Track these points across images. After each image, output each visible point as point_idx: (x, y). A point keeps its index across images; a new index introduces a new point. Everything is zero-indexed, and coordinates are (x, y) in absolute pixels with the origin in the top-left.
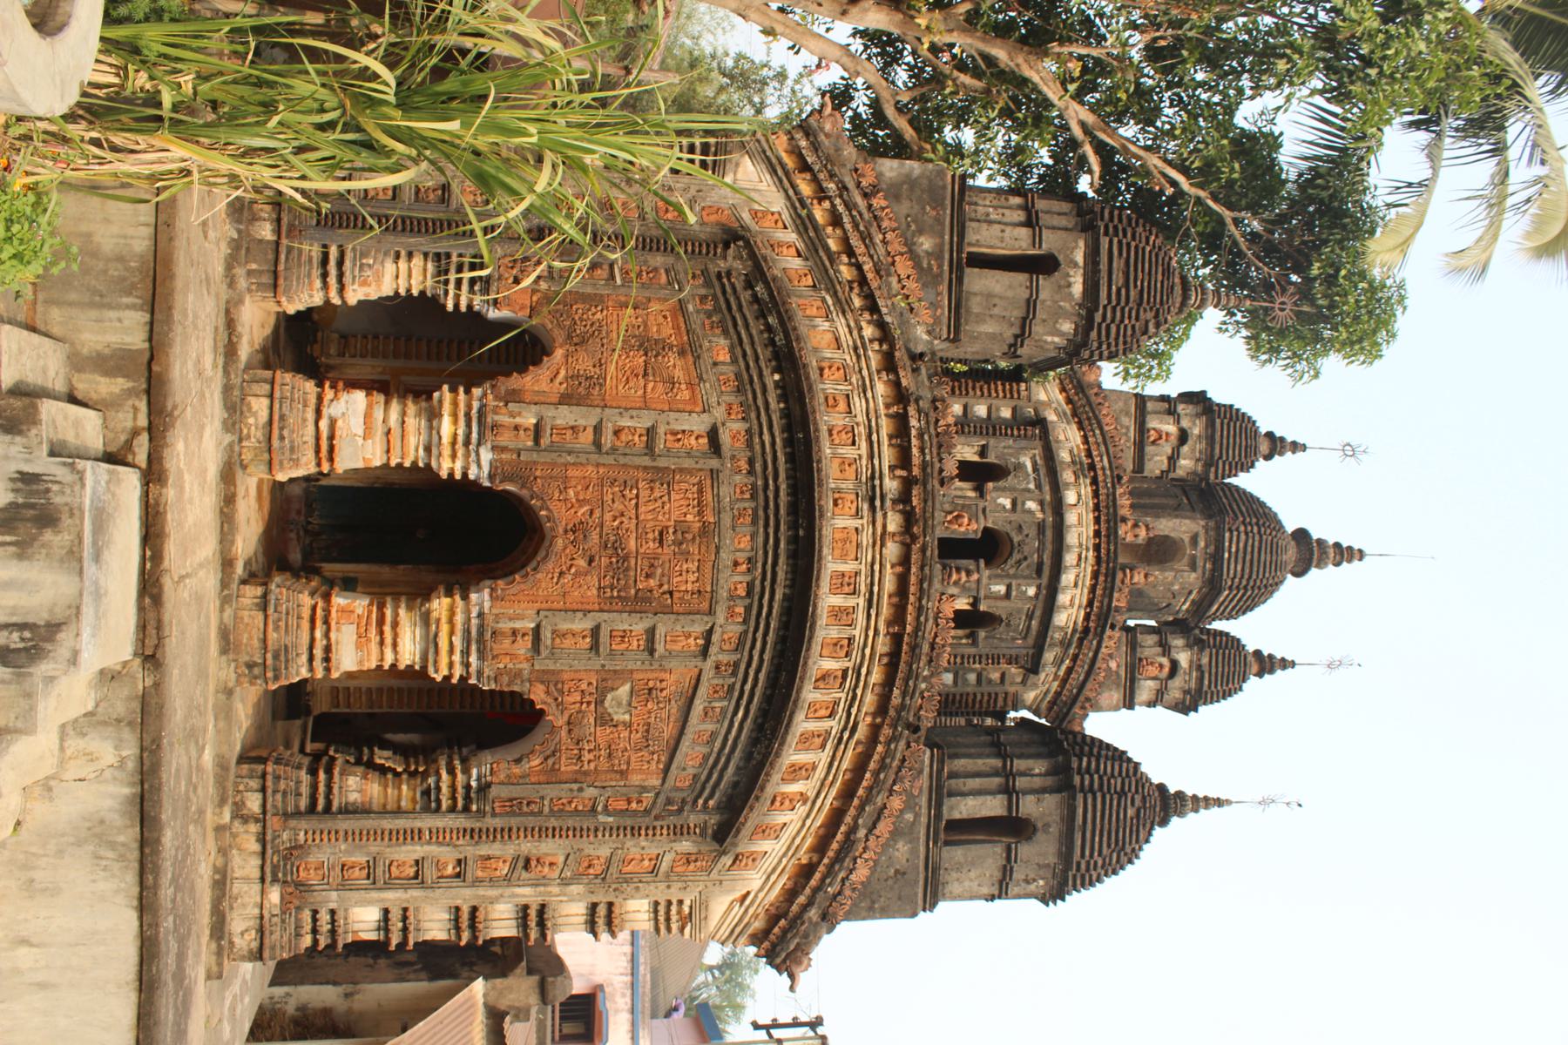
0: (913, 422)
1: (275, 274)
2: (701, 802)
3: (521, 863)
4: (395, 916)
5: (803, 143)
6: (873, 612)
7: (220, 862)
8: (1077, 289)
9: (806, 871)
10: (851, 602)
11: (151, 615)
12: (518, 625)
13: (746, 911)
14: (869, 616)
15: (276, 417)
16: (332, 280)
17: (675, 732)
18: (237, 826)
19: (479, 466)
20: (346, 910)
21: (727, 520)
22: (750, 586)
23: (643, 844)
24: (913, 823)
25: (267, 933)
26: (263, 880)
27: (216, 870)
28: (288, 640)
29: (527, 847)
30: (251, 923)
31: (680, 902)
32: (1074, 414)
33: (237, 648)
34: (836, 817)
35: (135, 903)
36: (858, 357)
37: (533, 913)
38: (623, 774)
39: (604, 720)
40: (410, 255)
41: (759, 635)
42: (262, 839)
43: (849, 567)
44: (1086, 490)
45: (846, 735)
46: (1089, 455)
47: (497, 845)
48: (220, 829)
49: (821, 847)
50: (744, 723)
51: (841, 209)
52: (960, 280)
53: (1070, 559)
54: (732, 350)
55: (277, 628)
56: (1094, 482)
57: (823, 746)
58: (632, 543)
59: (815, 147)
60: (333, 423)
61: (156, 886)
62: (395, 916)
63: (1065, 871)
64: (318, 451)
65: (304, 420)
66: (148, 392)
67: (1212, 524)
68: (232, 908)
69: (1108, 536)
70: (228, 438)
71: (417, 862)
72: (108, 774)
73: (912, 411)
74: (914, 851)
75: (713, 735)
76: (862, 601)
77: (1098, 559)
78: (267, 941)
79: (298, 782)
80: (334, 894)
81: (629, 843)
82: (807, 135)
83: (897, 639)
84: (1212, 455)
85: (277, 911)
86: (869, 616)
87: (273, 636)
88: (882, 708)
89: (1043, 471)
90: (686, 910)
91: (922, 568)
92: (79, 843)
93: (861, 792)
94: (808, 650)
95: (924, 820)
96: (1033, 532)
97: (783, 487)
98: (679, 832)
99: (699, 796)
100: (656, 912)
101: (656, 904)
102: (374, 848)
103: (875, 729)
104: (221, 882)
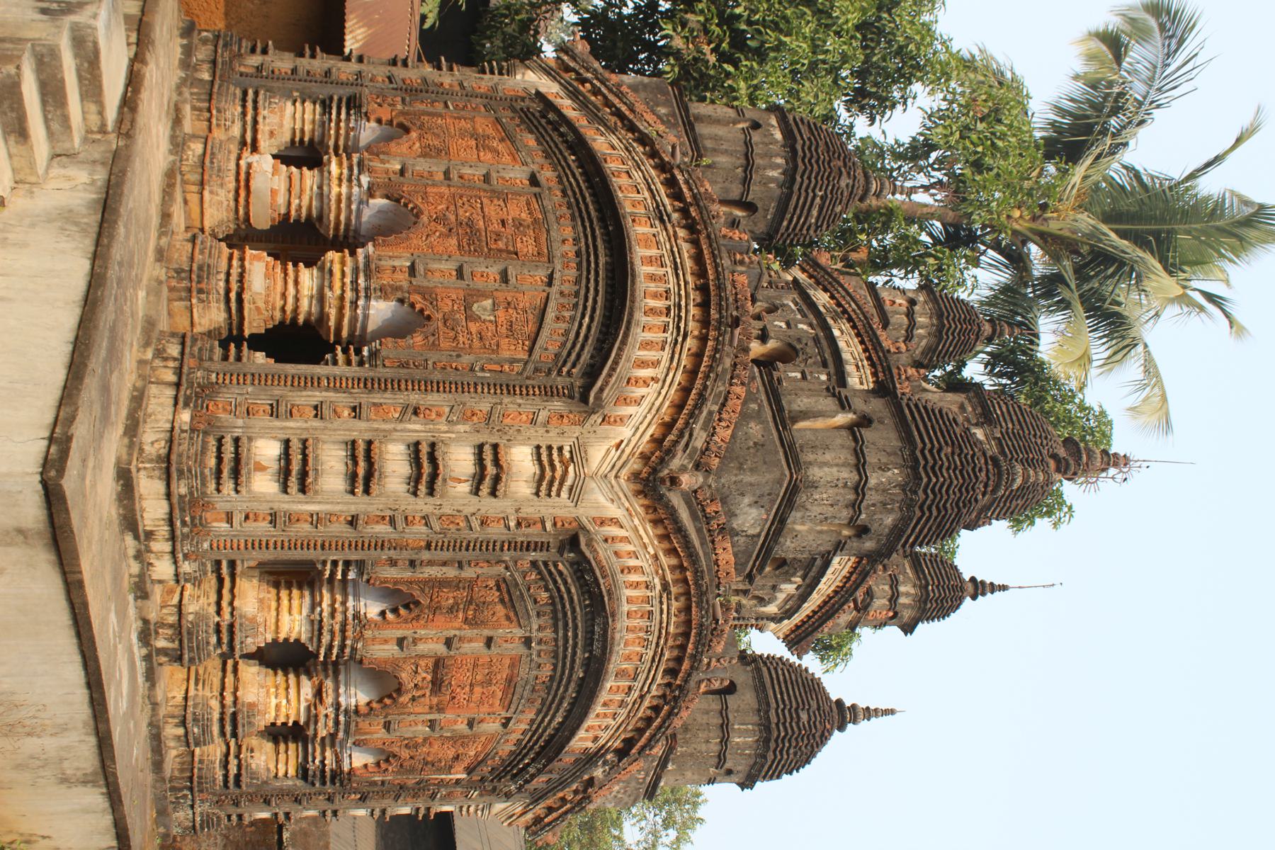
0: (679, 177)
1: (211, 95)
2: (565, 370)
3: (410, 410)
4: (296, 446)
5: (565, 58)
6: (680, 273)
7: (139, 384)
8: (778, 136)
9: (668, 427)
10: (661, 271)
11: (128, 116)
12: (397, 263)
13: (623, 451)
14: (677, 275)
15: (209, 151)
16: (250, 105)
17: (534, 329)
18: (158, 363)
19: (360, 186)
20: (250, 439)
21: (551, 217)
22: (578, 254)
23: (520, 401)
24: (759, 411)
25: (176, 442)
26: (176, 404)
27: (135, 388)
28: (211, 262)
29: (414, 398)
30: (162, 435)
31: (560, 449)
32: (818, 283)
33: (169, 260)
34: (685, 391)
35: (90, 255)
36: (630, 152)
37: (424, 449)
38: (496, 352)
39: (470, 317)
40: (303, 102)
41: (592, 277)
42: (179, 372)
43: (654, 252)
44: (846, 326)
45: (680, 339)
46: (839, 305)
47: (388, 395)
48: (142, 363)
49: (679, 407)
50: (591, 324)
51: (598, 84)
52: (693, 129)
53: (850, 368)
54: (537, 140)
55: (202, 252)
56: (850, 320)
57: (663, 349)
58: (481, 223)
59: (574, 58)
60: (249, 166)
61: (109, 246)
62: (296, 446)
63: (913, 453)
64: (237, 180)
65: (229, 160)
66: (139, 31)
67: (971, 394)
68: (145, 422)
69: (875, 349)
70: (172, 158)
71: (316, 407)
72: (80, 187)
73: (676, 172)
74: (766, 429)
75: (567, 332)
76: (669, 270)
77: (873, 365)
78: (175, 448)
79: (212, 350)
80: (240, 422)
81: (506, 400)
82: (567, 53)
83: (703, 289)
84: (940, 309)
85: (186, 427)
86: (677, 275)
87: (198, 257)
88: (705, 322)
89: (804, 308)
90: (567, 455)
91: (711, 246)
92: (50, 221)
93: (702, 369)
94: (633, 283)
95: (765, 403)
96: (811, 343)
97: (593, 213)
98: (549, 392)
99: (564, 365)
100: (539, 455)
101: (538, 447)
102: (277, 392)
103: (703, 339)
104: (138, 399)
